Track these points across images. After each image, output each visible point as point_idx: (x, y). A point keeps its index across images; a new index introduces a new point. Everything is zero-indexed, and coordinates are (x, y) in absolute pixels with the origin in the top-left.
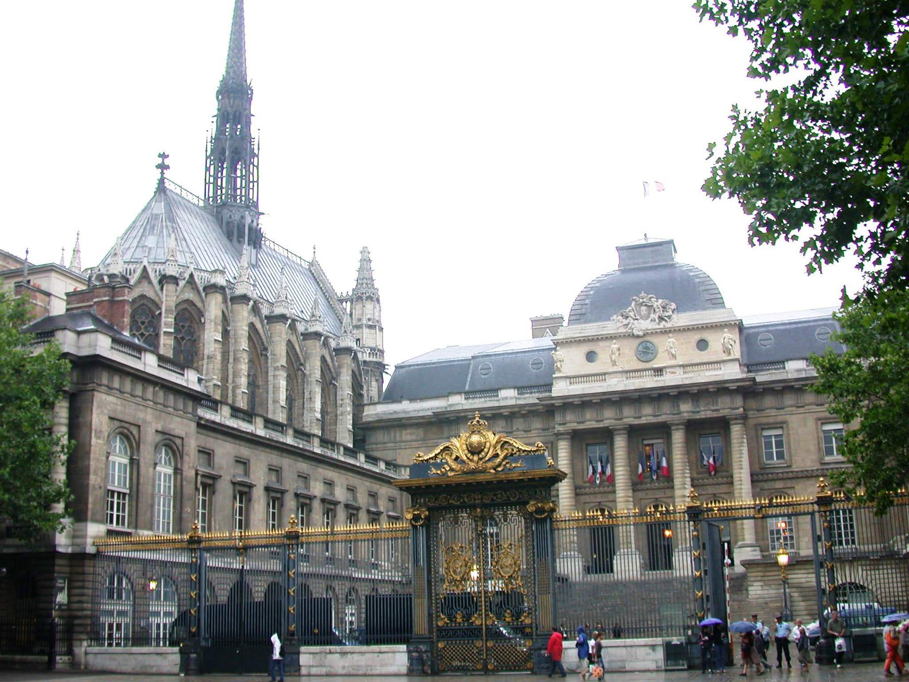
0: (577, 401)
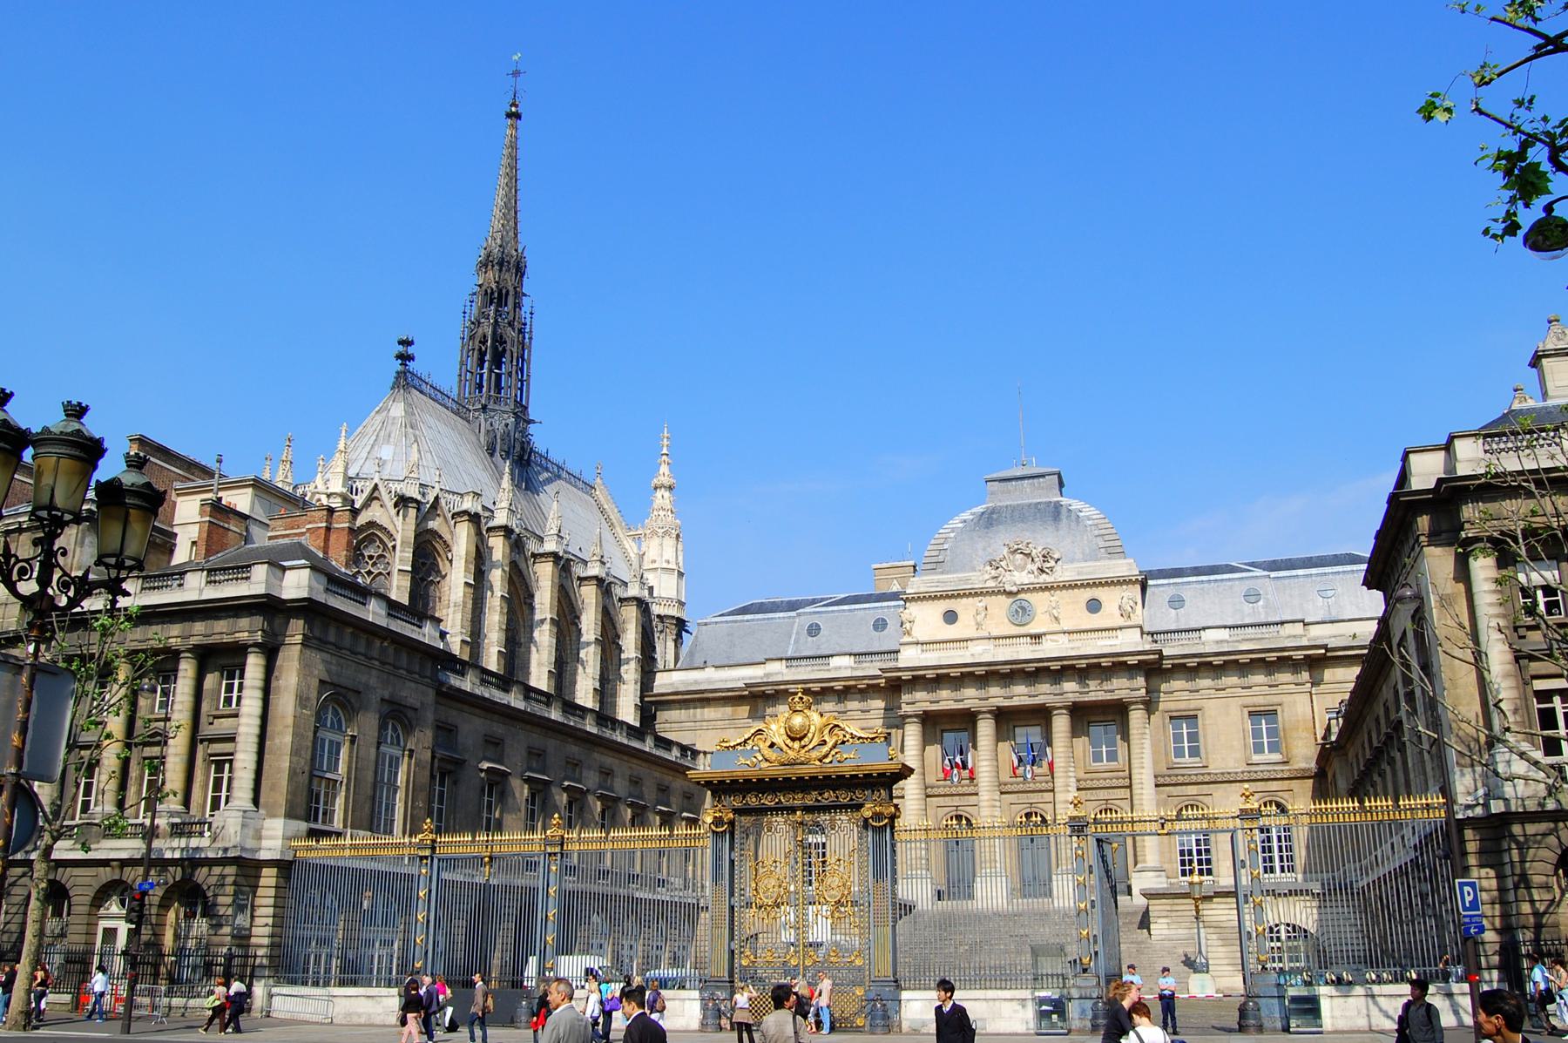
0: (930, 674)
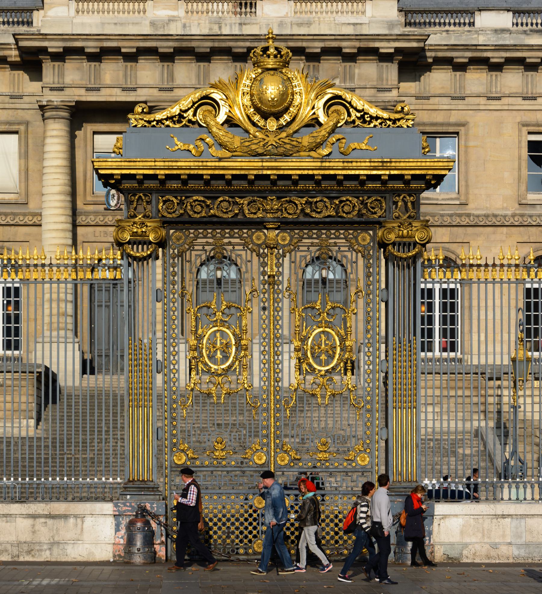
0: (92, 47)
